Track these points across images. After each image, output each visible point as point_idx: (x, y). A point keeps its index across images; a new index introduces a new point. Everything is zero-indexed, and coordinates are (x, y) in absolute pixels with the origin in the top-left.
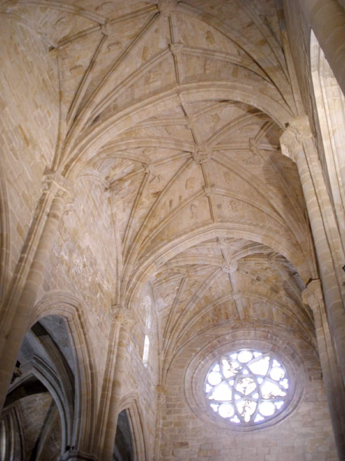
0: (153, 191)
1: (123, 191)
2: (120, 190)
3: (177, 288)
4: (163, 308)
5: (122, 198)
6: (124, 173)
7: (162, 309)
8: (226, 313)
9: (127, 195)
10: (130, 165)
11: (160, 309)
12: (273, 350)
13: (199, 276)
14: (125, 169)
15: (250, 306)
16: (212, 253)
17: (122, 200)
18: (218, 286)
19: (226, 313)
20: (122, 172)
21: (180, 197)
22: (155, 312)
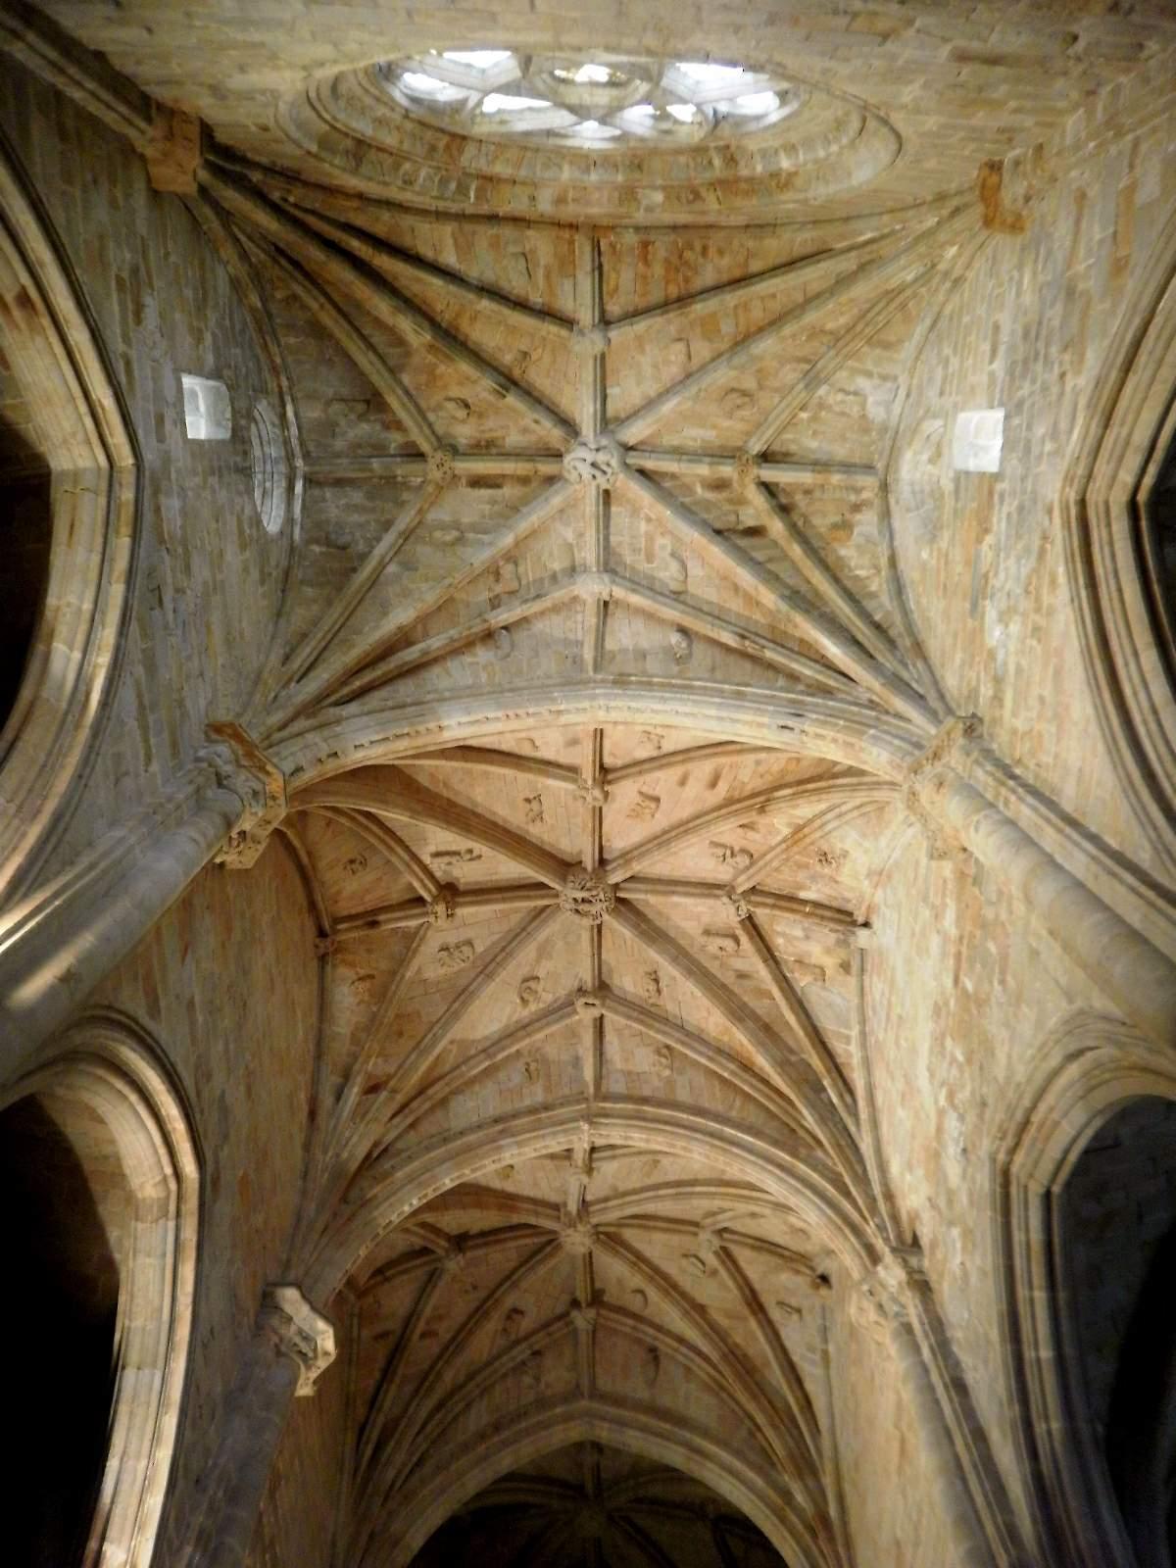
0: (751, 834)
1: (827, 890)
2: (836, 898)
3: (804, 415)
4: (876, 381)
5: (836, 882)
6: (804, 929)
7: (884, 378)
8: (646, 262)
9: (822, 876)
10: (783, 935)
11: (889, 385)
12: (460, 140)
13: (714, 427)
14: (796, 938)
15: (547, 277)
16: (643, 527)
17: (839, 879)
18: (655, 366)
19: (646, 262)
20: (807, 937)
21: (683, 782)
22: (908, 395)
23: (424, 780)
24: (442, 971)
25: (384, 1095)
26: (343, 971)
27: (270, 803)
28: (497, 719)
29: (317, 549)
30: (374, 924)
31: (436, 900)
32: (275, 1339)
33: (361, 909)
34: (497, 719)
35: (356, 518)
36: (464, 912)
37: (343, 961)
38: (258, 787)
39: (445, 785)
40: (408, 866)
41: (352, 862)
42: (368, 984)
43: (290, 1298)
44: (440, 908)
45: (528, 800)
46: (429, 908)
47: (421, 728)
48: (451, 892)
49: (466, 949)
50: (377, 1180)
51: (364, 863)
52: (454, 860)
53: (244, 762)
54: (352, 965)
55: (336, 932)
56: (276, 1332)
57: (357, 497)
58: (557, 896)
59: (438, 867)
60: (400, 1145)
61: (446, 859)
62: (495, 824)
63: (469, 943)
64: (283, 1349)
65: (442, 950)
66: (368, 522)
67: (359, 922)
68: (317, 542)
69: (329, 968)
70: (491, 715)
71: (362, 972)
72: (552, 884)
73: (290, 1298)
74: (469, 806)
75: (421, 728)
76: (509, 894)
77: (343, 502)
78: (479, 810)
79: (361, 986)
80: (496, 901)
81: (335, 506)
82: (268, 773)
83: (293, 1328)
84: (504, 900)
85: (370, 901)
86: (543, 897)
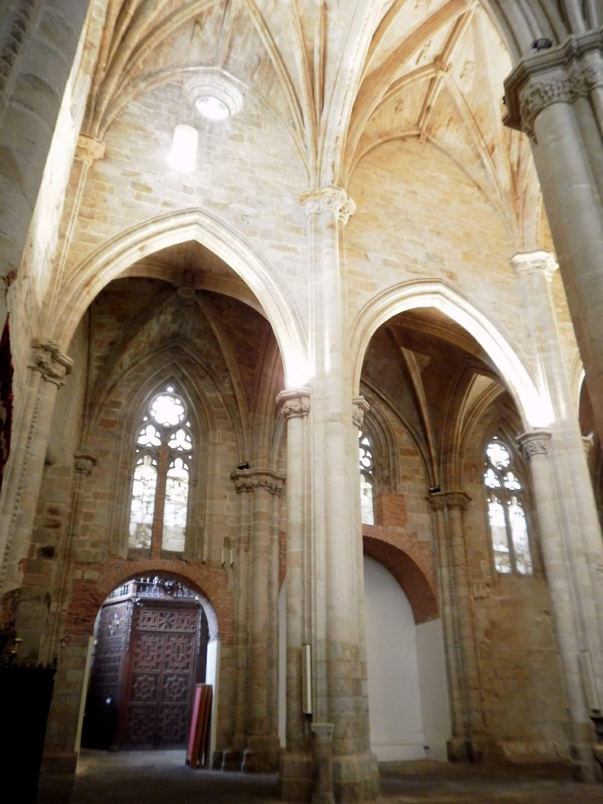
23: (377, 65)
24: (470, 83)
25: (496, 149)
26: (439, 132)
27: (336, 196)
28: (362, 37)
29: (256, 76)
30: (429, 108)
31: (436, 72)
32: (525, 273)
33: (420, 109)
34: (362, 37)
35: (249, 46)
36: (451, 59)
37: (436, 130)
38: (326, 200)
39: (386, 52)
40: (413, 81)
41: (396, 109)
42: (452, 123)
43: (518, 258)
44: (441, 74)
45: (416, 7)
46: (439, 77)
47: (347, 82)
48: (439, 61)
49: (469, 66)
50: (523, 177)
51: (401, 101)
52: (423, 55)
53: (317, 198)
54: (440, 126)
55: (420, 129)
56: (523, 271)
57: (239, 41)
58: (470, 12)
59: (423, 62)
60: (522, 153)
61: (422, 59)
62: (418, 29)
63: (467, 63)
64: (530, 272)
65: (461, 77)
66: (252, 41)
67: (424, 116)
68: (253, 74)
69: (434, 140)
70: (358, 40)
71: (446, 123)
72: (463, 12)
73: (518, 258)
74: (402, 41)
75: (347, 82)
76: (456, 34)
77: (239, 50)
78: (407, 36)
79: (450, 128)
80: (455, 41)
81: (240, 57)
82: (325, 192)
83: (529, 264)
84: (457, 38)
85: (419, 104)
86: (467, 17)
